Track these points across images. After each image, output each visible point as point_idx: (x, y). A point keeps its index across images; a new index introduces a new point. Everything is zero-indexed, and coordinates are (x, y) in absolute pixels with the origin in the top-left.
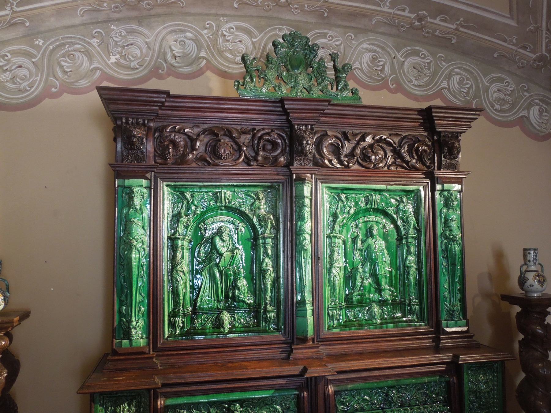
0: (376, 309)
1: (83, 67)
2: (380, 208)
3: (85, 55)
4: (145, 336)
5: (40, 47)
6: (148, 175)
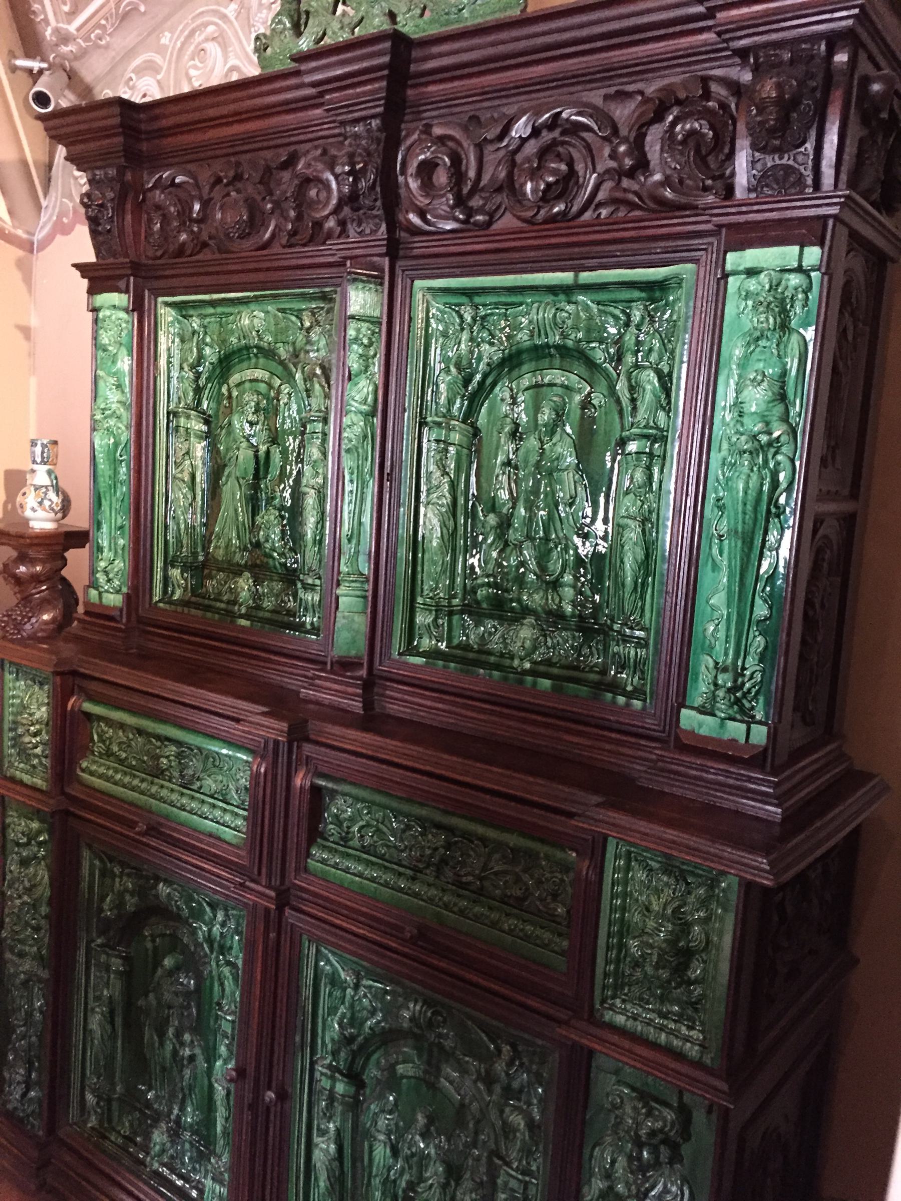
1: (216, 71)
2: (570, 343)
3: (219, 43)
4: (125, 590)
5: (165, 47)
6: (122, 284)
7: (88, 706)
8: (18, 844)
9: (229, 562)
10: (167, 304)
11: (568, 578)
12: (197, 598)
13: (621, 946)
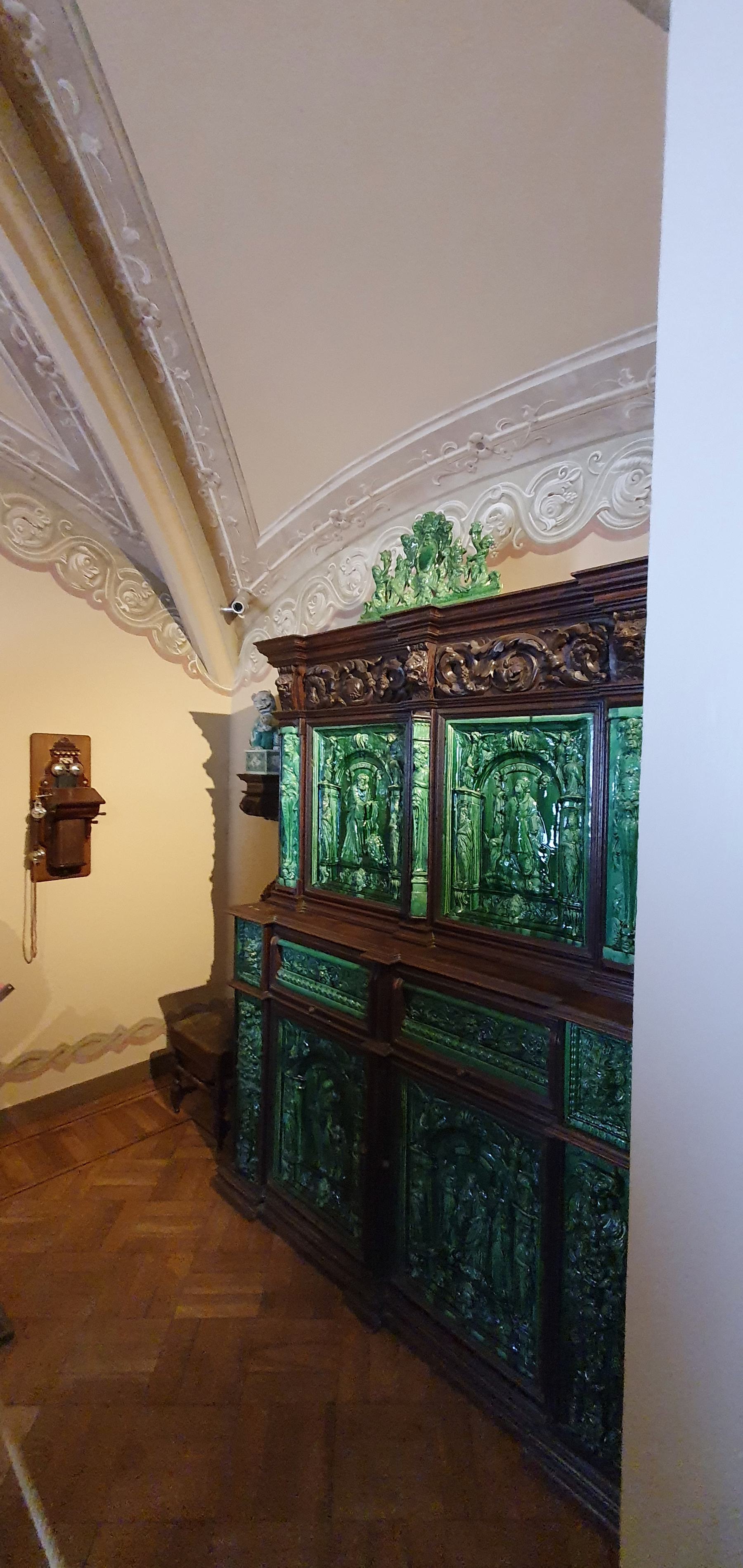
0: (516, 902)
2: (530, 750)
6: (295, 722)
7: (281, 942)
8: (246, 1017)
9: (352, 863)
10: (316, 731)
11: (536, 873)
12: (334, 883)
13: (577, 1082)
